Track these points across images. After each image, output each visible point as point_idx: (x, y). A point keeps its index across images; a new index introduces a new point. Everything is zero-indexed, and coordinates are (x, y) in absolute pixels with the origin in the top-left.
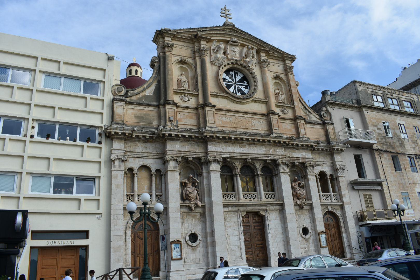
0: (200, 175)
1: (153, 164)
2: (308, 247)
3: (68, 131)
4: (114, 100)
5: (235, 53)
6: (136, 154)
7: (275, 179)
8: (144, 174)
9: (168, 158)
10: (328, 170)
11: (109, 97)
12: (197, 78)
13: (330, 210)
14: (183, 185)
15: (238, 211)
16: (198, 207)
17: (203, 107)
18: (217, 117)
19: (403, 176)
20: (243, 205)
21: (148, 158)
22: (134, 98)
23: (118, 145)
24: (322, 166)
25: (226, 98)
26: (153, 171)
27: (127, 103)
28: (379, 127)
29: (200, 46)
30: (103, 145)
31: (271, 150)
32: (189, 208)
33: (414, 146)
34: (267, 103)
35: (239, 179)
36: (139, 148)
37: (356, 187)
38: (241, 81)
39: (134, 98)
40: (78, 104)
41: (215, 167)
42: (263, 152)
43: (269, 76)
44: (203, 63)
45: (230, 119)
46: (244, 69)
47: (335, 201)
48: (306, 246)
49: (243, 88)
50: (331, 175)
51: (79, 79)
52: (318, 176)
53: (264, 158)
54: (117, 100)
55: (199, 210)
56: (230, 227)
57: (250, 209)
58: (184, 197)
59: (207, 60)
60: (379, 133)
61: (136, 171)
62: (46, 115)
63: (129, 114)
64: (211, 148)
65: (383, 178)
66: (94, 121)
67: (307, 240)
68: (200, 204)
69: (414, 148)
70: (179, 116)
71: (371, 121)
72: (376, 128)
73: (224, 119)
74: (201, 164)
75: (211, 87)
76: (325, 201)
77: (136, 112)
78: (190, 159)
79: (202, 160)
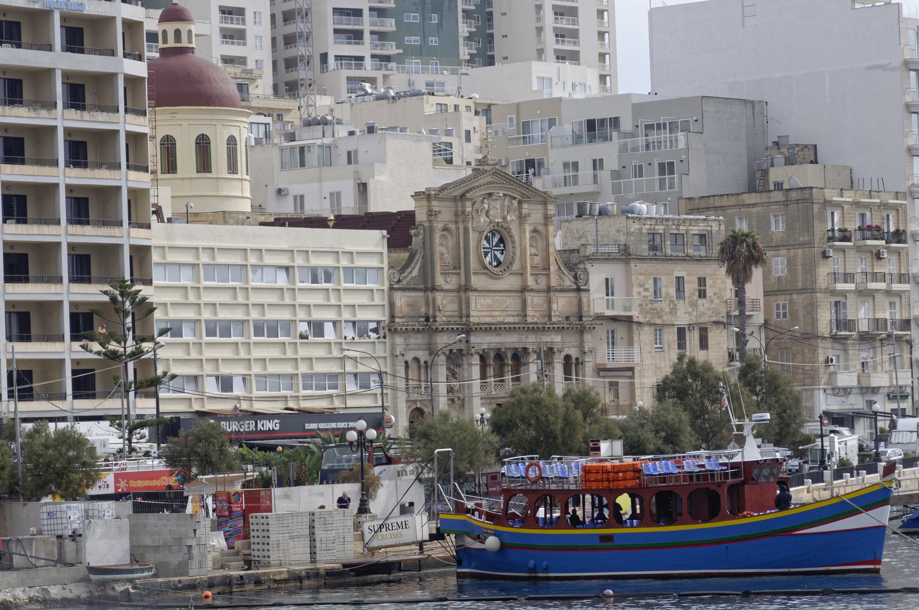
0: (459, 366)
1: (423, 356)
4: (391, 289)
10: (574, 353)
15: (490, 403)
20: (494, 398)
21: (419, 350)
22: (404, 282)
23: (399, 340)
25: (485, 274)
26: (422, 363)
28: (646, 286)
29: (464, 207)
30: (387, 340)
33: (690, 310)
37: (601, 374)
41: (476, 360)
44: (466, 230)
45: (488, 301)
46: (503, 231)
49: (499, 255)
50: (577, 359)
60: (645, 297)
61: (410, 363)
64: (473, 339)
65: (637, 360)
69: (690, 314)
72: (642, 289)
73: (482, 301)
75: (474, 264)
78: (455, 351)
79: (464, 352)
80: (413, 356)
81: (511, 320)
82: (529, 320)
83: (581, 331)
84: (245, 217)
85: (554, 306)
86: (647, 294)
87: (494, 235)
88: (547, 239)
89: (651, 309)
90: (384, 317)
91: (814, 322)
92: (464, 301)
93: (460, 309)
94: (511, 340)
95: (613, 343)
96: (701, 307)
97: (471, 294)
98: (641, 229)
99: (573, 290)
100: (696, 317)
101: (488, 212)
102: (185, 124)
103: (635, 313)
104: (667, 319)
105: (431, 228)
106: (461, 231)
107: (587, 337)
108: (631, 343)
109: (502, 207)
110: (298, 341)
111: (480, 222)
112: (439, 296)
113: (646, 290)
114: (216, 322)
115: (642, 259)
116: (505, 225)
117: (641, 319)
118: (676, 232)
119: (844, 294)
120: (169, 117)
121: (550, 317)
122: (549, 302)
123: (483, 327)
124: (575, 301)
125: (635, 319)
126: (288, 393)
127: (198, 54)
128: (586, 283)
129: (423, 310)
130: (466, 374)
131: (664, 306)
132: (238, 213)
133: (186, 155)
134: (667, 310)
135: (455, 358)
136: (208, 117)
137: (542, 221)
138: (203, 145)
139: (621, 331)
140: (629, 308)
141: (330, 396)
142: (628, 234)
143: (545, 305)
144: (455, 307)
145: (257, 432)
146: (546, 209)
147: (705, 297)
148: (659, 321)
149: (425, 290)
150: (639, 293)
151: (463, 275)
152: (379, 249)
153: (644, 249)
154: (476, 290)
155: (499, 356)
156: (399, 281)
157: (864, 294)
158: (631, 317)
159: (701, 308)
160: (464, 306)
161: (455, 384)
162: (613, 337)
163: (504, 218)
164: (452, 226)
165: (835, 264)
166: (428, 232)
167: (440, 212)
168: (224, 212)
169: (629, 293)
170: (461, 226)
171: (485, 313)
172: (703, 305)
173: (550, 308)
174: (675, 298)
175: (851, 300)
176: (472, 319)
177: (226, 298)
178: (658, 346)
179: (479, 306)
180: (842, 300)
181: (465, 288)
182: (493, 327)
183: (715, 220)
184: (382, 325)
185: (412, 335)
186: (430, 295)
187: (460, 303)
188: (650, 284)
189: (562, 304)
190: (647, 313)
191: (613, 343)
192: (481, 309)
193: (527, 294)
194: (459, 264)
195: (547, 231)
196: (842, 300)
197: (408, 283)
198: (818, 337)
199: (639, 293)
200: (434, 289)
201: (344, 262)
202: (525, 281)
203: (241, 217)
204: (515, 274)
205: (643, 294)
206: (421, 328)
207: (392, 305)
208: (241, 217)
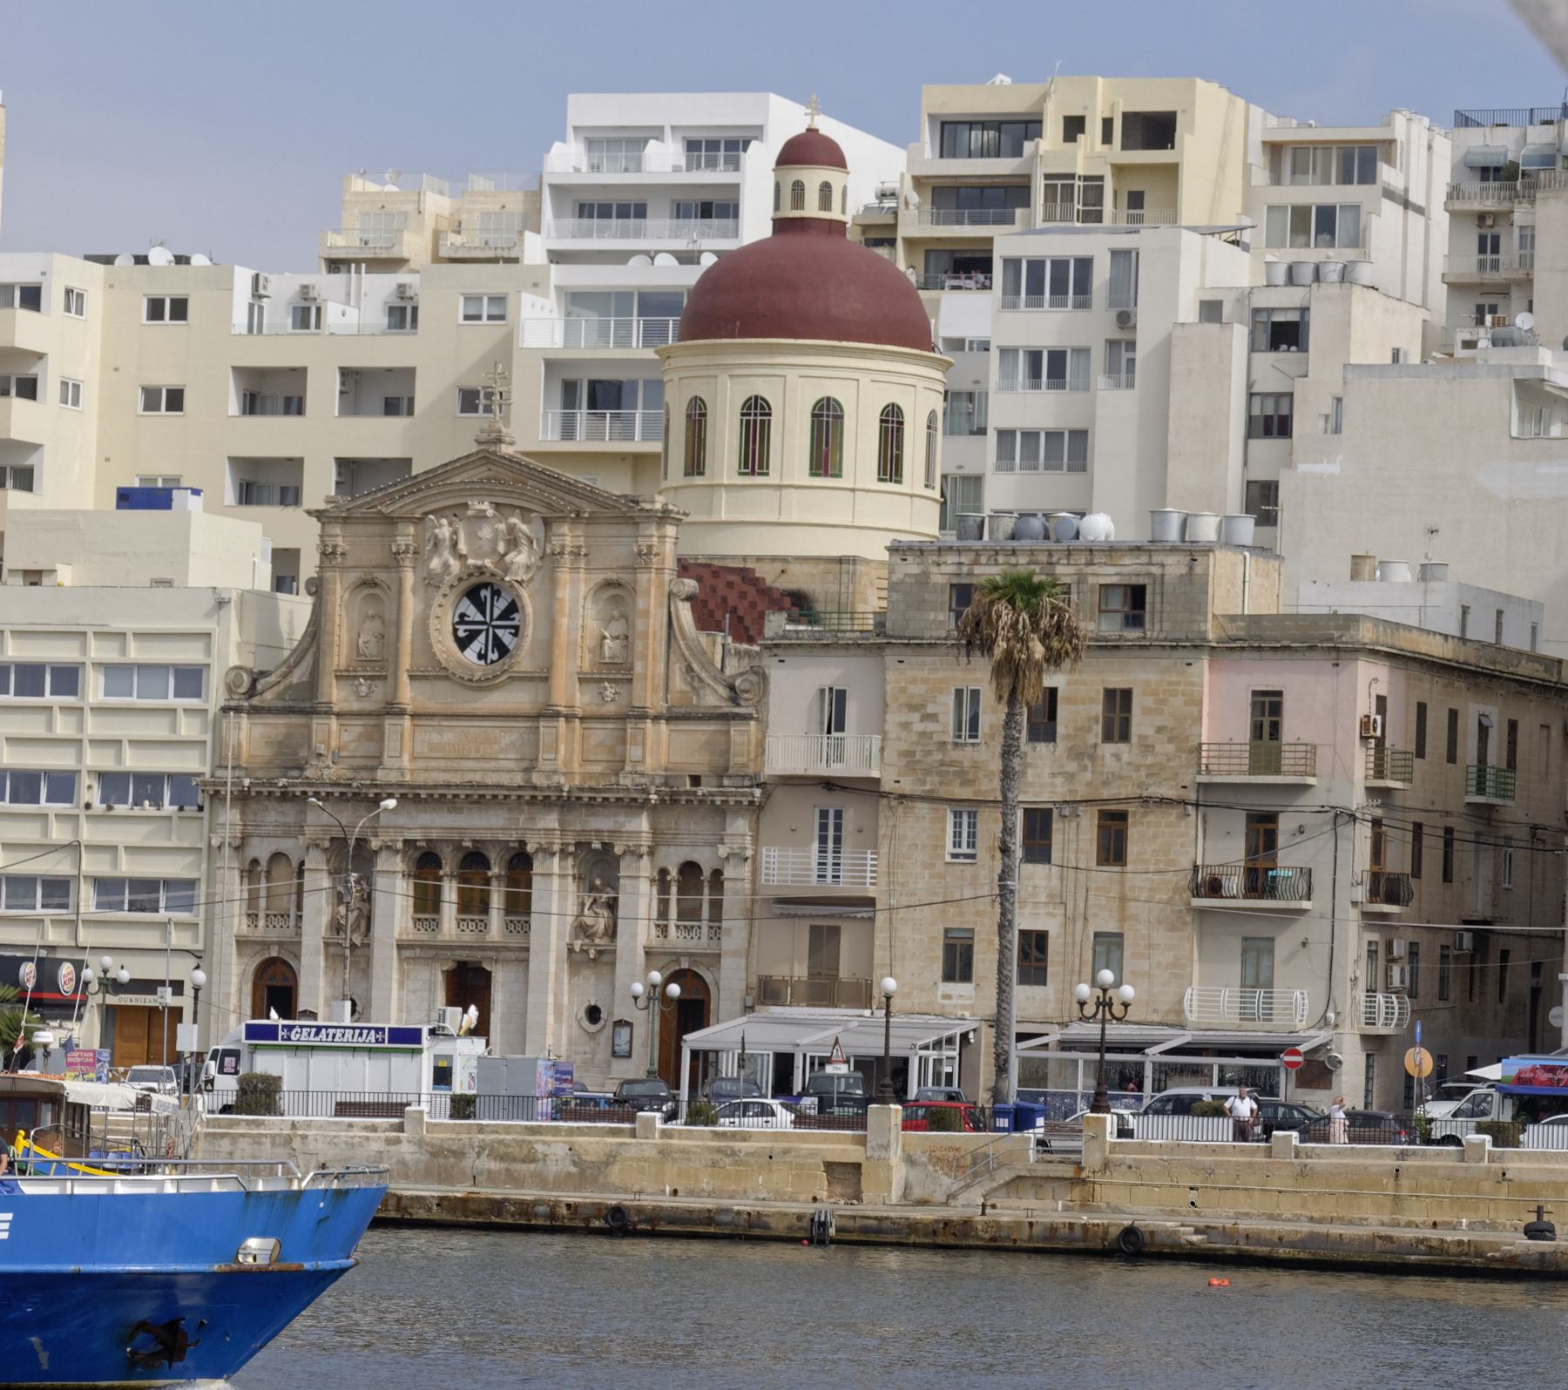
2: (594, 1053)
3: (149, 785)
6: (263, 830)
10: (705, 859)
13: (685, 965)
16: (352, 947)
22: (269, 695)
24: (694, 845)
25: (447, 678)
27: (255, 711)
28: (930, 709)
30: (206, 814)
31: (522, 817)
33: (1072, 766)
36: (273, 816)
40: (157, 729)
48: (588, 1049)
51: (163, 668)
52: (674, 873)
53: (502, 837)
56: (415, 991)
57: (463, 955)
59: (409, 578)
60: (923, 734)
62: (107, 762)
66: (189, 762)
67: (592, 1036)
69: (1070, 777)
71: (903, 690)
72: (916, 717)
73: (435, 737)
81: (505, 779)
82: (537, 779)
85: (634, 752)
86: (931, 727)
87: (496, 593)
89: (942, 763)
95: (837, 840)
96: (1109, 760)
98: (926, 574)
100: (1089, 784)
101: (455, 545)
113: (932, 717)
115: (918, 646)
117: (907, 786)
125: (887, 786)
147: (1125, 737)
150: (906, 726)
155: (474, 860)
156: (252, 692)
158: (877, 781)
159: (1110, 764)
162: (838, 827)
164: (381, 576)
171: (442, 764)
172: (1117, 757)
178: (964, 849)
185: (272, 805)
189: (661, 750)
190: (928, 772)
191: (837, 840)
197: (280, 696)
199: (906, 726)
205: (919, 727)
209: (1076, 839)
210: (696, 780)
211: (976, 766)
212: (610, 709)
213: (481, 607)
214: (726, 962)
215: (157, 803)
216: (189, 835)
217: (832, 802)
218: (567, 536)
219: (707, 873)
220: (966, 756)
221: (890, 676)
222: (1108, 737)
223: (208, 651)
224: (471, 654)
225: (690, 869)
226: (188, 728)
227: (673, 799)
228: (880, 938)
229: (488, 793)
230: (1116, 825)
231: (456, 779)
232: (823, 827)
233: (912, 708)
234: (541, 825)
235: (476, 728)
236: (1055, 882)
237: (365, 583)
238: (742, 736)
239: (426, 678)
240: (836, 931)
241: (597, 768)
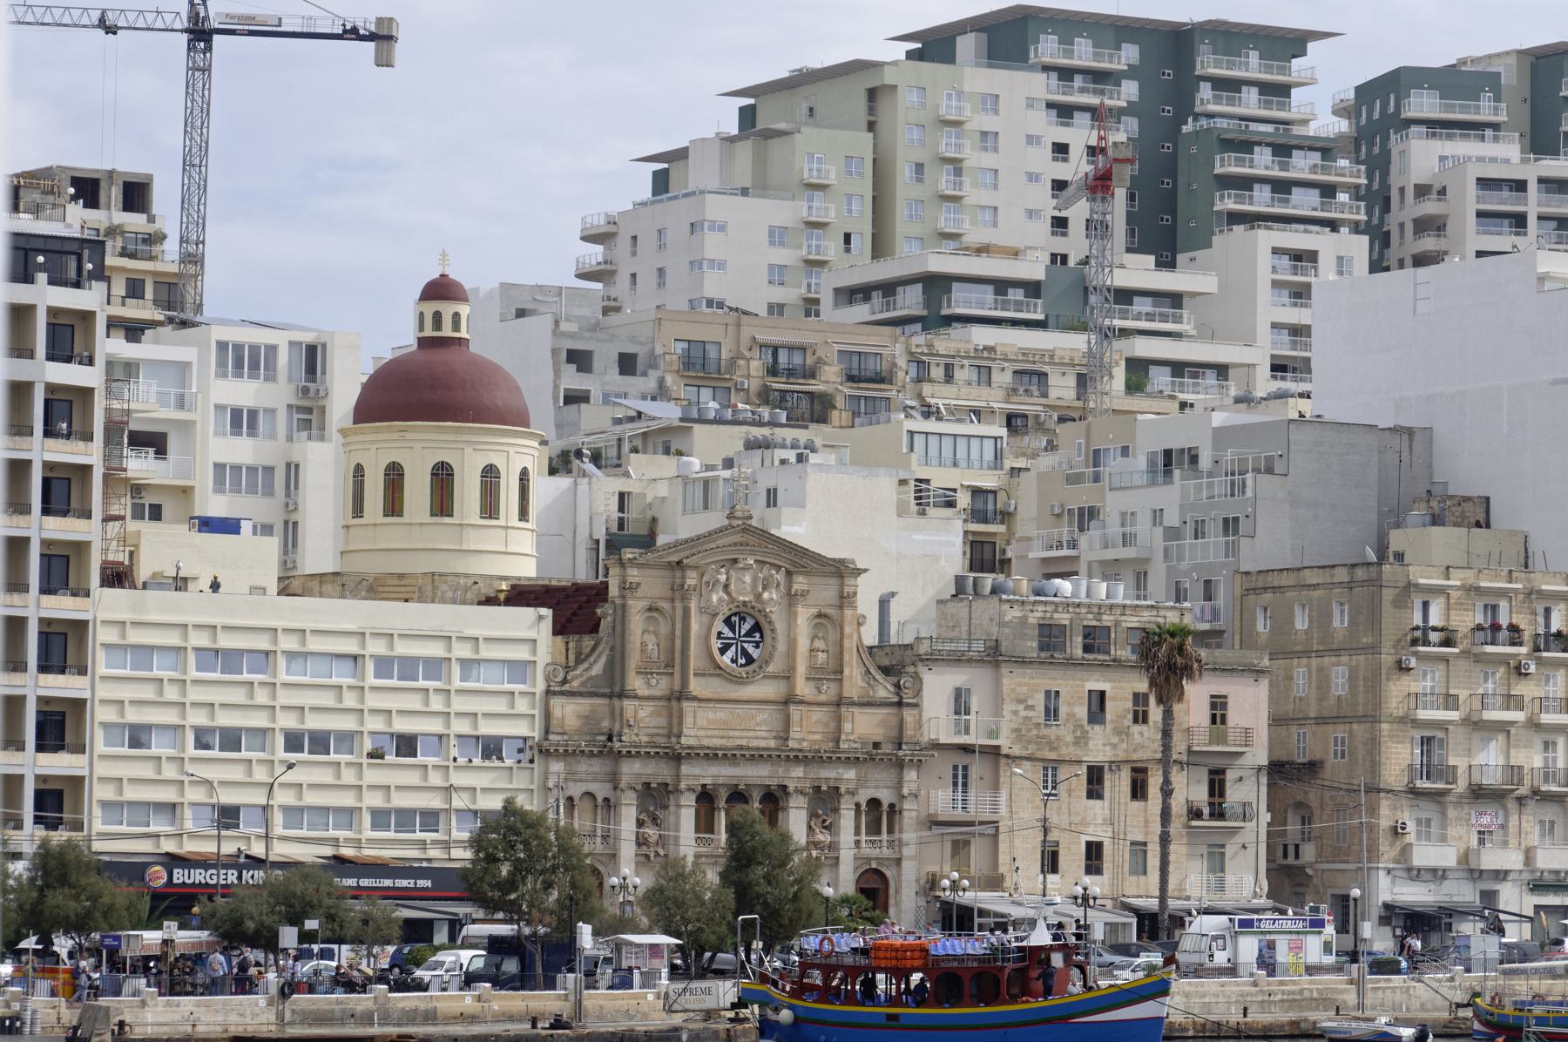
0: (665, 807)
1: (601, 790)
4: (549, 693)
5: (744, 585)
7: (780, 815)
8: (587, 804)
9: (623, 784)
10: (886, 797)
11: (540, 687)
12: (673, 641)
13: (874, 866)
14: (640, 823)
17: (679, 699)
18: (700, 713)
19: (1059, 809)
21: (594, 780)
22: (575, 684)
23: (557, 767)
24: (877, 787)
26: (600, 800)
28: (1030, 702)
29: (683, 578)
30: (535, 765)
32: (647, 857)
33: (1115, 740)
34: (788, 676)
35: (723, 814)
36: (583, 767)
38: (749, 634)
39: (575, 684)
42: (766, 773)
43: (804, 615)
44: (686, 611)
45: (721, 715)
46: (757, 615)
47: (886, 852)
49: (750, 649)
50: (892, 806)
52: (863, 807)
54: (555, 693)
55: (659, 859)
58: (641, 842)
59: (693, 606)
61: (576, 801)
63: (568, 712)
64: (685, 769)
65: (1003, 810)
68: (662, 852)
69: (1114, 746)
70: (642, 714)
71: (1013, 690)
72: (1021, 707)
73: (711, 715)
74: (669, 792)
75: (695, 659)
76: (867, 851)
77: (578, 708)
80: (584, 789)
81: (763, 744)
82: (792, 744)
83: (900, 765)
84: (470, 582)
85: (847, 727)
86: (1031, 714)
87: (742, 619)
88: (842, 628)
90: (536, 734)
91: (1375, 767)
92: (675, 714)
93: (670, 725)
94: (758, 774)
95: (965, 785)
96: (1137, 736)
97: (685, 704)
98: (1025, 617)
99: (891, 704)
101: (726, 586)
102: (418, 446)
103: (1004, 742)
104: (1068, 752)
105: (624, 607)
106: (679, 613)
107: (911, 775)
108: (996, 787)
109: (755, 580)
110: (365, 761)
111: (709, 600)
112: (629, 706)
113: (1031, 708)
114: (212, 730)
115: (1023, 662)
116: (759, 606)
118: (1094, 623)
119: (1443, 725)
120: (396, 436)
121: (837, 741)
122: (839, 720)
123: (702, 753)
124: (894, 721)
125: (1005, 751)
126: (342, 834)
127: (474, 348)
128: (918, 693)
129: (605, 724)
130: (672, 819)
131: (1063, 732)
132: (457, 575)
133: (417, 491)
134: (1070, 738)
135: (655, 798)
136: (452, 437)
137: (836, 602)
138: (443, 477)
139: (978, 768)
140: (994, 733)
141: (423, 844)
142: (1001, 624)
143: (833, 725)
144: (662, 721)
145: (394, 888)
146: (842, 585)
148: (1053, 756)
149: (611, 697)
150: (1015, 713)
151: (677, 676)
152: (532, 634)
153: (1031, 646)
154: (695, 699)
156: (565, 681)
157: (1476, 725)
158: (998, 747)
160: (675, 721)
161: (651, 832)
162: (965, 776)
163: (758, 596)
164: (665, 605)
165: (1424, 681)
166: (619, 612)
167: (638, 584)
168: (433, 574)
169: (997, 711)
170: (678, 605)
172: (1141, 734)
173: (839, 730)
174: (1085, 722)
175: (1456, 736)
176: (683, 740)
177: (327, 699)
179: (700, 722)
180: (1440, 734)
181: (680, 695)
182: (720, 753)
183: (1172, 608)
184: (529, 743)
185: (583, 760)
186: (616, 702)
187: (670, 716)
188: (1039, 701)
189: (864, 726)
190: (1029, 742)
191: (965, 785)
192: (700, 726)
193: (792, 707)
194: (673, 659)
195: (842, 615)
196: (1440, 734)
197: (583, 684)
198: (1379, 790)
199: (1015, 713)
200: (622, 695)
201: (462, 651)
202: (792, 687)
203: (462, 581)
204: (775, 677)
205: (1023, 714)
206: (596, 750)
207: (547, 715)
208: (462, 581)
209: (1118, 784)
210: (876, 745)
211: (1058, 738)
212: (823, 698)
213: (732, 628)
214: (905, 863)
215: (500, 758)
216: (521, 781)
217: (962, 760)
218: (800, 583)
219: (885, 807)
220: (1052, 732)
221: (1005, 681)
222: (1136, 721)
223: (534, 652)
224: (726, 659)
225: (874, 803)
226: (522, 706)
227: (870, 756)
228: (1003, 847)
229: (765, 753)
230: (1140, 776)
231: (730, 743)
232: (955, 776)
233: (1020, 701)
234: (794, 774)
235: (740, 710)
236: (1107, 811)
237: (650, 609)
238: (909, 715)
239: (703, 675)
240: (967, 843)
241: (817, 737)
